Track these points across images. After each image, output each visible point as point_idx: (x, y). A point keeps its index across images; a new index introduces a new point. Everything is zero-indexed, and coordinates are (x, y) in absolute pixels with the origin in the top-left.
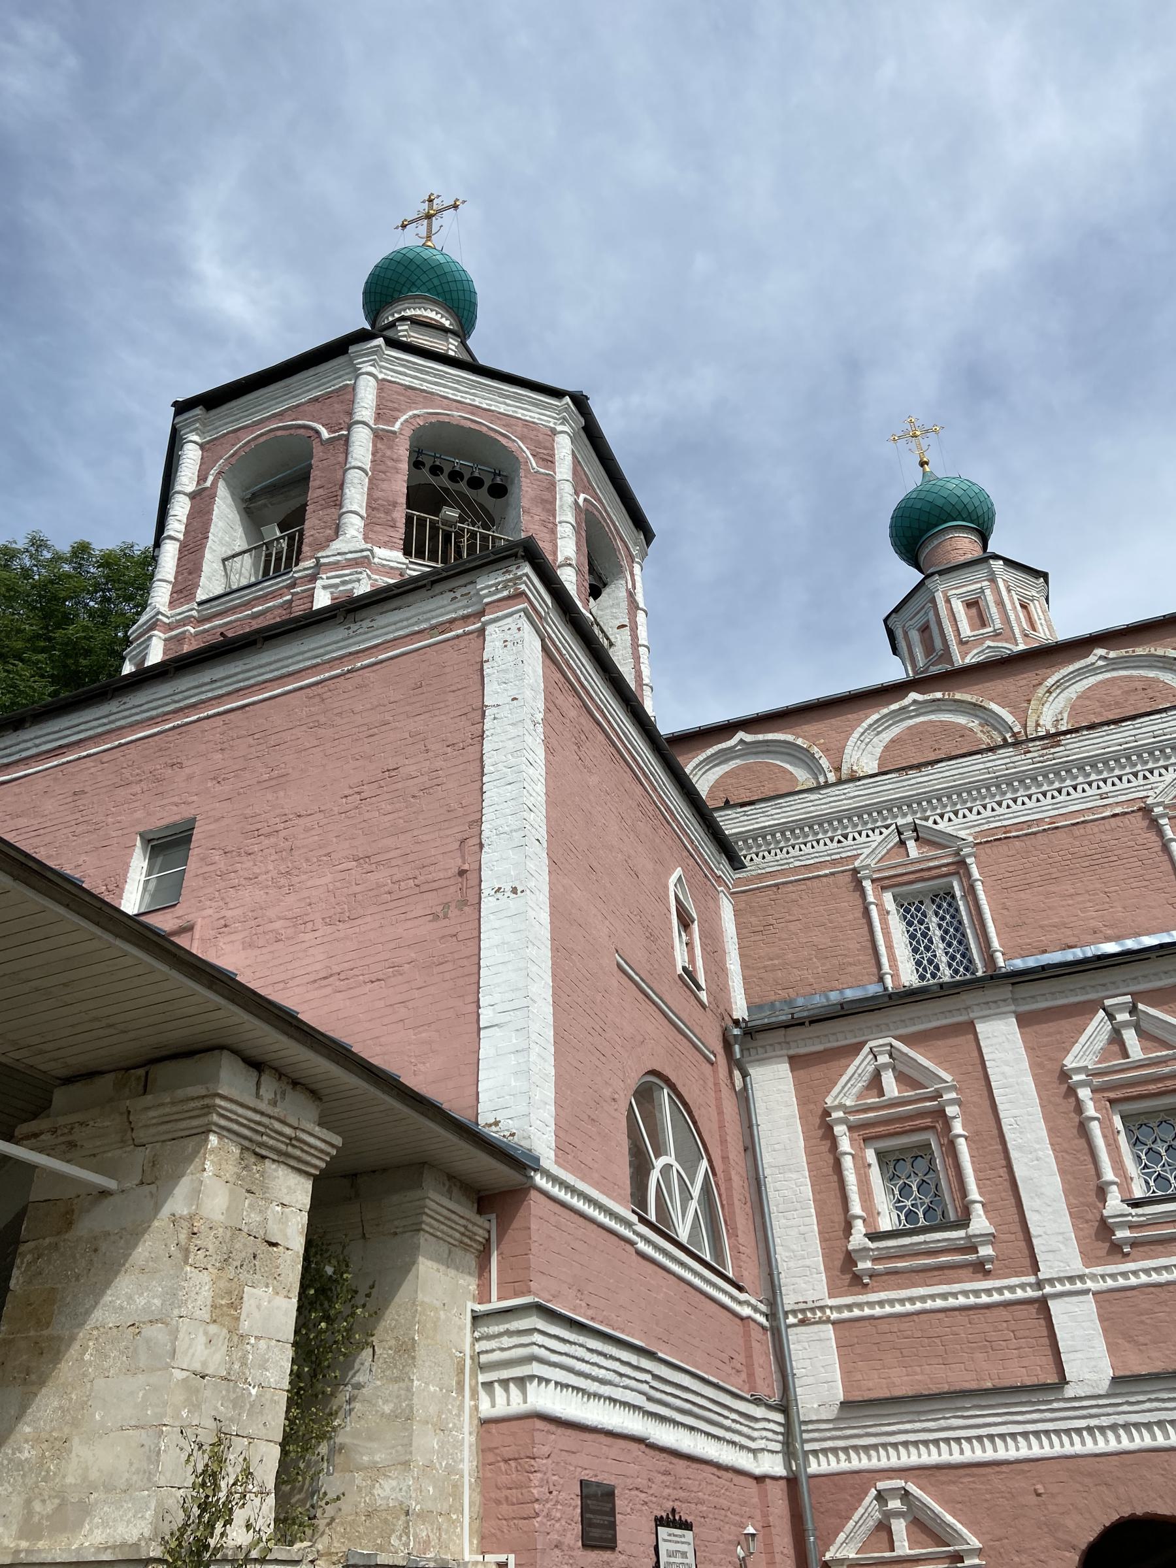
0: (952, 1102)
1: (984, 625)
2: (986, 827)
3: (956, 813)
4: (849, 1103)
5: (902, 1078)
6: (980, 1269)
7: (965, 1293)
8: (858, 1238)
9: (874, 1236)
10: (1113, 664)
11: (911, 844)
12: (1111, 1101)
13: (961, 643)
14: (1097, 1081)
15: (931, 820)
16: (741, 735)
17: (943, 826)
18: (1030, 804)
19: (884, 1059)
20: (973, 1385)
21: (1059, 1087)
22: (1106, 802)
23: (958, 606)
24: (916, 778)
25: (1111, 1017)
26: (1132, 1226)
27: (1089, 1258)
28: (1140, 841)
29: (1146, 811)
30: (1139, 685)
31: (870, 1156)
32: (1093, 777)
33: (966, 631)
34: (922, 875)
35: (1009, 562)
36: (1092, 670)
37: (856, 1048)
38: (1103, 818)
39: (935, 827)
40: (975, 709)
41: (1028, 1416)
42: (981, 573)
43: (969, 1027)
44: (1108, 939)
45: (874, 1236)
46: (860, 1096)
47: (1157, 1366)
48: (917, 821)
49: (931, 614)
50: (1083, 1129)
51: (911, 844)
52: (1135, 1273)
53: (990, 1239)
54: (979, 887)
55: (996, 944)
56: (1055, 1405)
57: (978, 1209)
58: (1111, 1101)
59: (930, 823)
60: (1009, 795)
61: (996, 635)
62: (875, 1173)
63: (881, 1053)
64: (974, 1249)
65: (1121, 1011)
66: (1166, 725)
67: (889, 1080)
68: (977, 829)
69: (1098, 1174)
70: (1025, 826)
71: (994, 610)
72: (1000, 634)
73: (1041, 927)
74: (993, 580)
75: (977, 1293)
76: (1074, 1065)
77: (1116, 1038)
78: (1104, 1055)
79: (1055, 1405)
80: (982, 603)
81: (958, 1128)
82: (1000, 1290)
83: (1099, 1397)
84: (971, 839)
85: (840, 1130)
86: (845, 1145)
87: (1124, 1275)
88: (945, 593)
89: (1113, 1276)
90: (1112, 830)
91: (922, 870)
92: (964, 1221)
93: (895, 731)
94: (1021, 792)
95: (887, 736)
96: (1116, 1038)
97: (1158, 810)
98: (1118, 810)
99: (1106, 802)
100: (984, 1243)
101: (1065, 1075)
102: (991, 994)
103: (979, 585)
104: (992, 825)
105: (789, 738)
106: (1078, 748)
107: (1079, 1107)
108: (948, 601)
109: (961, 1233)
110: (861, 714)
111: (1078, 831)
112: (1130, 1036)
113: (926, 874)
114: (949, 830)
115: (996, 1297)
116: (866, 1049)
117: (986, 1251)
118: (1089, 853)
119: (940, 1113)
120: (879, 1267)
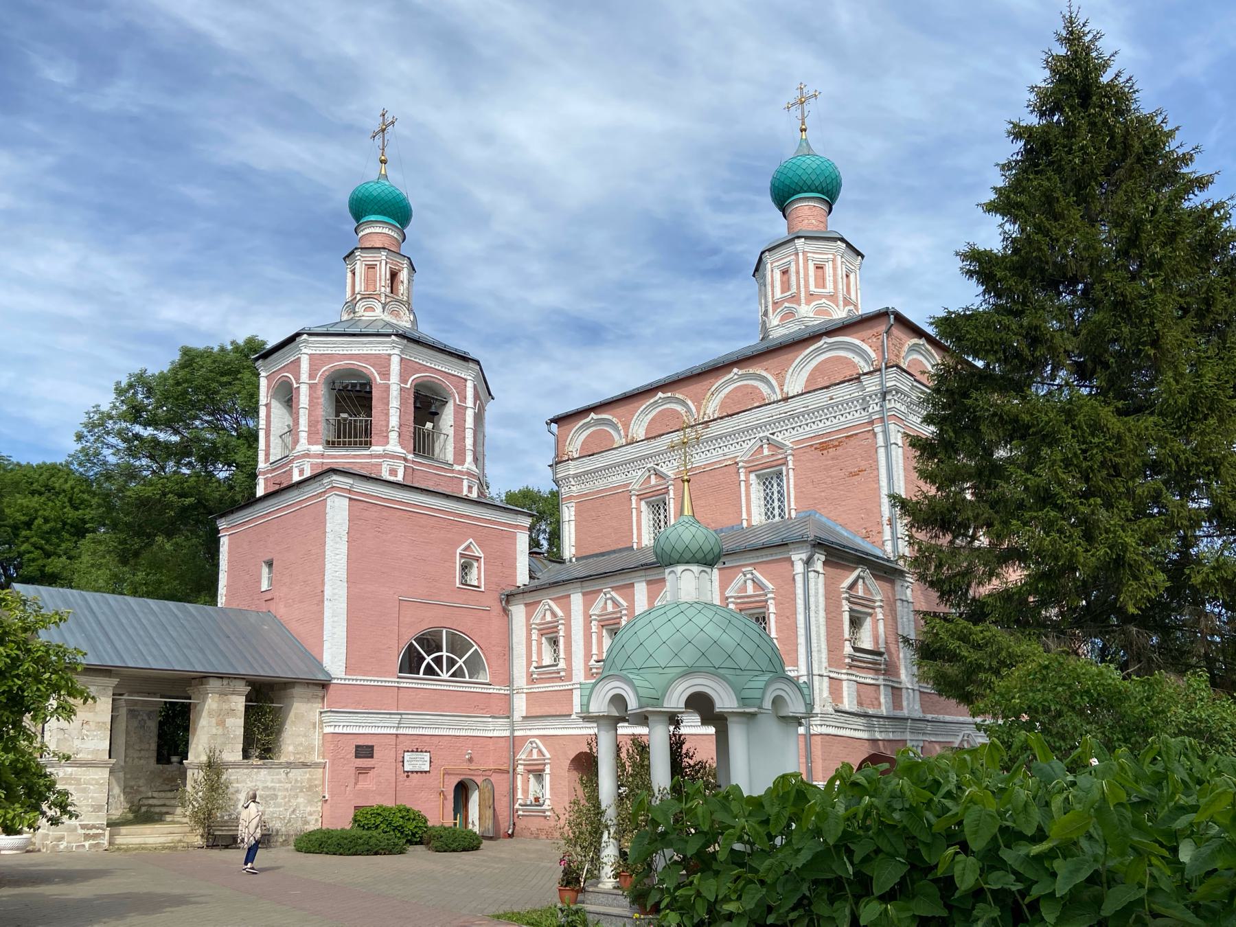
10: (741, 377)
11: (653, 477)
13: (775, 303)
16: (592, 415)
23: (777, 275)
30: (750, 390)
33: (778, 295)
36: (732, 381)
40: (683, 403)
42: (789, 249)
43: (569, 596)
51: (653, 477)
93: (654, 413)
95: (650, 416)
105: (610, 417)
110: (636, 405)
111: (712, 473)
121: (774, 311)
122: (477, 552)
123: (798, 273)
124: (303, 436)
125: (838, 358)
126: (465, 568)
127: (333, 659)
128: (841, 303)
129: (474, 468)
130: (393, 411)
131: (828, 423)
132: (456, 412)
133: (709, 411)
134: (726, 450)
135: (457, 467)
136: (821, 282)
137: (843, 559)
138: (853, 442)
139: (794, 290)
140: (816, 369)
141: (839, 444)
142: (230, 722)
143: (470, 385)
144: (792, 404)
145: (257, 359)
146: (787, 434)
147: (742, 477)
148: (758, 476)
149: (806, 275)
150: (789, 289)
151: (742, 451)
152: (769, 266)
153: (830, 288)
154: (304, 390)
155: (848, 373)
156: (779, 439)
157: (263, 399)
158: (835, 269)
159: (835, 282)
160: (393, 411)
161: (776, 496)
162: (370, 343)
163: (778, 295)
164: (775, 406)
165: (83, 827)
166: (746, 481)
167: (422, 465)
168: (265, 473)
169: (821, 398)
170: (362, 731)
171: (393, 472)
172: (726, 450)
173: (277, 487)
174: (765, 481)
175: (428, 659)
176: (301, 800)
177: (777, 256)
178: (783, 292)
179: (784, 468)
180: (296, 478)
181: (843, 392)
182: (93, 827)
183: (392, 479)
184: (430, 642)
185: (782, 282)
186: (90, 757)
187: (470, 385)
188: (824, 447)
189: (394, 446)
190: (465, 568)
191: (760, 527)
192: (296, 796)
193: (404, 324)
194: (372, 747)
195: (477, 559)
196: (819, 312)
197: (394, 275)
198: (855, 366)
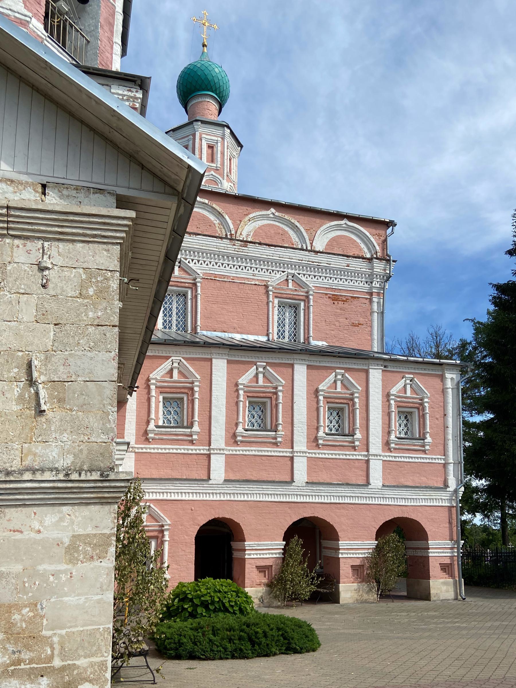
0: (197, 386)
1: (212, 161)
2: (208, 272)
3: (198, 261)
4: (158, 378)
5: (180, 372)
6: (192, 442)
7: (184, 449)
8: (152, 426)
9: (157, 427)
12: (248, 396)
14: (246, 389)
15: (188, 260)
17: (191, 265)
18: (228, 268)
19: (176, 365)
20: (180, 477)
21: (234, 387)
22: (254, 277)
25: (257, 369)
26: (243, 436)
27: (227, 444)
28: (260, 298)
29: (266, 286)
31: (161, 398)
32: (253, 265)
35: (232, 133)
37: (167, 358)
38: (251, 284)
39: (188, 264)
41: (196, 487)
44: (238, 333)
45: (157, 427)
46: (163, 376)
47: (237, 478)
48: (182, 259)
49: (191, 142)
50: (237, 404)
52: (239, 450)
53: (198, 433)
54: (199, 297)
55: (199, 323)
56: (205, 485)
57: (196, 424)
58: (248, 396)
59: (187, 262)
60: (221, 261)
61: (216, 170)
62: (161, 404)
63: (176, 362)
64: (191, 436)
65: (261, 367)
66: (285, 254)
67: (175, 373)
68: (205, 272)
69: (237, 419)
70: (223, 277)
71: (219, 155)
72: (218, 170)
73: (217, 321)
74: (223, 139)
75: (188, 449)
76: (241, 382)
77: (256, 376)
78: (251, 381)
79: (205, 485)
80: (215, 149)
81: (197, 395)
82: (196, 450)
83: (219, 484)
84: (201, 275)
85: (153, 387)
86: (153, 393)
87: (236, 450)
88: (201, 136)
89: (232, 450)
90: (253, 290)
91: (178, 282)
92: (191, 426)
94: (226, 262)
96: (256, 376)
97: (270, 288)
98: (257, 283)
99: (254, 277)
100: (195, 434)
101: (237, 385)
102: (221, 351)
103: (216, 139)
104: (211, 272)
107: (238, 396)
108: (201, 140)
109: (189, 430)
111: (241, 286)
112: (261, 376)
113: (179, 284)
114: (194, 268)
115: (194, 452)
116: (170, 360)
117: (195, 437)
118: (242, 296)
119: (192, 389)
120: (157, 437)
131: (341, 283)
134: (256, 272)
138: (355, 302)
141: (345, 301)
146: (309, 279)
151: (275, 279)
156: (304, 279)
164: (307, 253)
166: (273, 303)
169: (339, 262)
172: (256, 272)
177: (206, 130)
179: (302, 304)
188: (335, 298)
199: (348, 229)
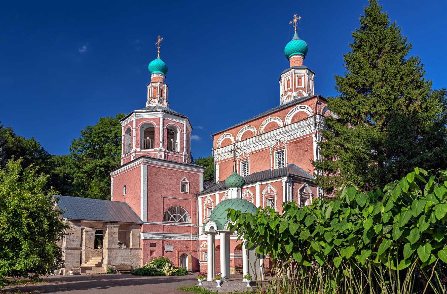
24: (244, 142)
33: (286, 89)
34: (244, 159)
106: (263, 137)
121: (285, 95)
122: (187, 181)
123: (292, 81)
124: (134, 146)
125: (301, 112)
126: (184, 186)
127: (142, 217)
128: (306, 91)
129: (186, 153)
130: (160, 136)
132: (180, 135)
133: (261, 131)
135: (181, 154)
136: (300, 84)
137: (299, 180)
138: (305, 141)
139: (291, 87)
140: (294, 116)
142: (114, 236)
143: (185, 126)
144: (287, 128)
145: (121, 121)
147: (271, 153)
148: (276, 153)
149: (295, 82)
150: (289, 87)
151: (271, 144)
152: (283, 79)
153: (303, 86)
154: (134, 130)
155: (305, 117)
157: (123, 134)
158: (305, 79)
159: (305, 83)
160: (160, 136)
161: (282, 160)
162: (154, 114)
163: (286, 89)
165: (74, 267)
167: (170, 153)
168: (123, 158)
169: (295, 126)
170: (152, 239)
171: (161, 156)
173: (127, 162)
174: (279, 153)
175: (172, 216)
176: (135, 260)
178: (288, 88)
180: (132, 159)
181: (302, 123)
182: (77, 267)
183: (160, 158)
184: (172, 210)
185: (287, 85)
186: (75, 247)
187: (185, 126)
188: (296, 143)
189: (161, 148)
190: (184, 186)
191: (277, 170)
192: (133, 259)
193: (164, 106)
194: (155, 244)
195: (187, 183)
196: (300, 94)
197: (162, 90)
198: (307, 114)
199: (300, 108)
